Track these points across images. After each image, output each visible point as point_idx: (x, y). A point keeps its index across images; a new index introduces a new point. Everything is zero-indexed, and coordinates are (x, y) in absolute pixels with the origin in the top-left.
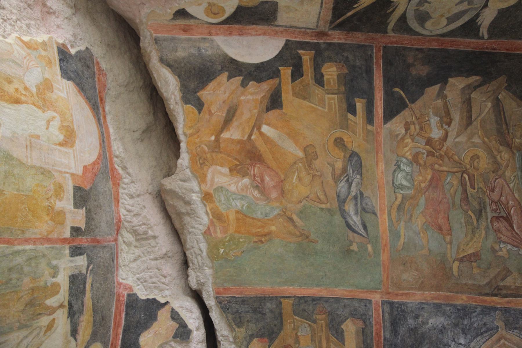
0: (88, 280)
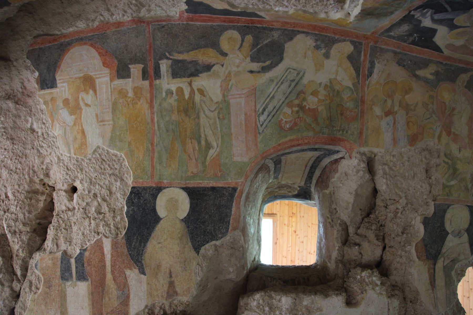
0: (176, 58)
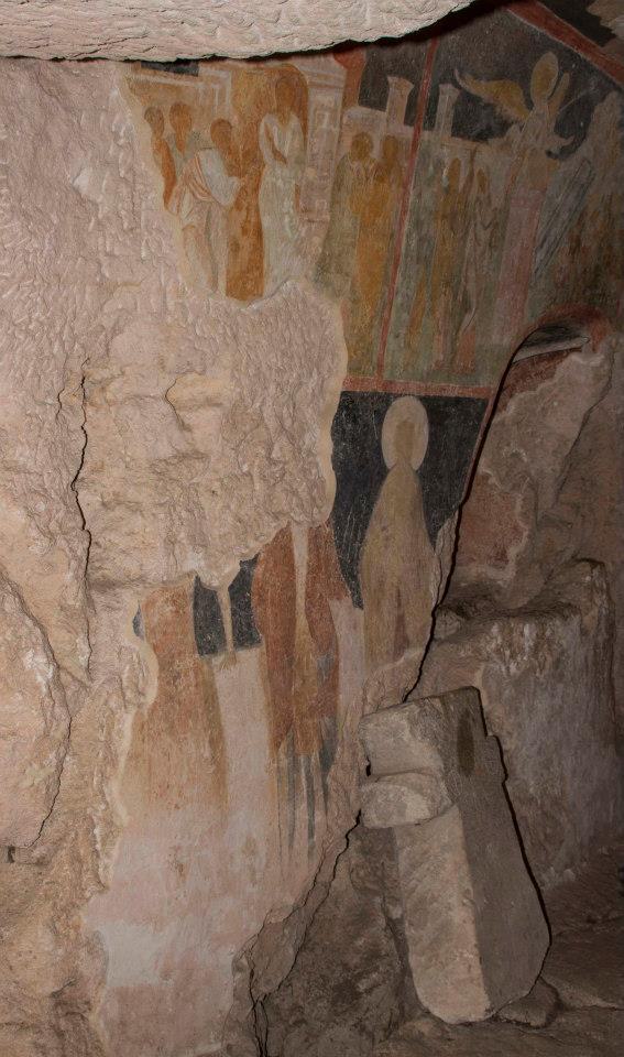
0: (467, 87)
